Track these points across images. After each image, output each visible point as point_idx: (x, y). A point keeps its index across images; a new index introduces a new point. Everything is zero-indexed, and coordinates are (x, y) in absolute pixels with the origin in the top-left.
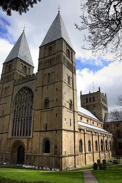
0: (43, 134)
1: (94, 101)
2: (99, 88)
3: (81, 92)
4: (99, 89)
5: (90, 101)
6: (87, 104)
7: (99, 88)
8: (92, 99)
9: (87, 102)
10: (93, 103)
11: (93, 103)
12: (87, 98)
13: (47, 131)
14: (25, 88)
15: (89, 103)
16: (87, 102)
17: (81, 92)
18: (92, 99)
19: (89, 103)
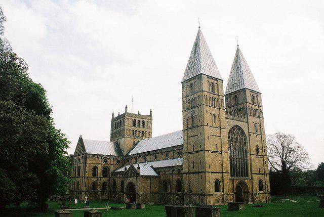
0: (258, 176)
1: (143, 127)
2: (151, 111)
3: (126, 107)
4: (151, 114)
5: (139, 126)
6: (134, 128)
7: (151, 111)
8: (141, 123)
9: (135, 125)
10: (141, 129)
11: (141, 129)
12: (135, 120)
13: (260, 174)
14: (237, 126)
15: (136, 128)
16: (135, 125)
17: (126, 107)
18: (141, 123)
19: (136, 128)
